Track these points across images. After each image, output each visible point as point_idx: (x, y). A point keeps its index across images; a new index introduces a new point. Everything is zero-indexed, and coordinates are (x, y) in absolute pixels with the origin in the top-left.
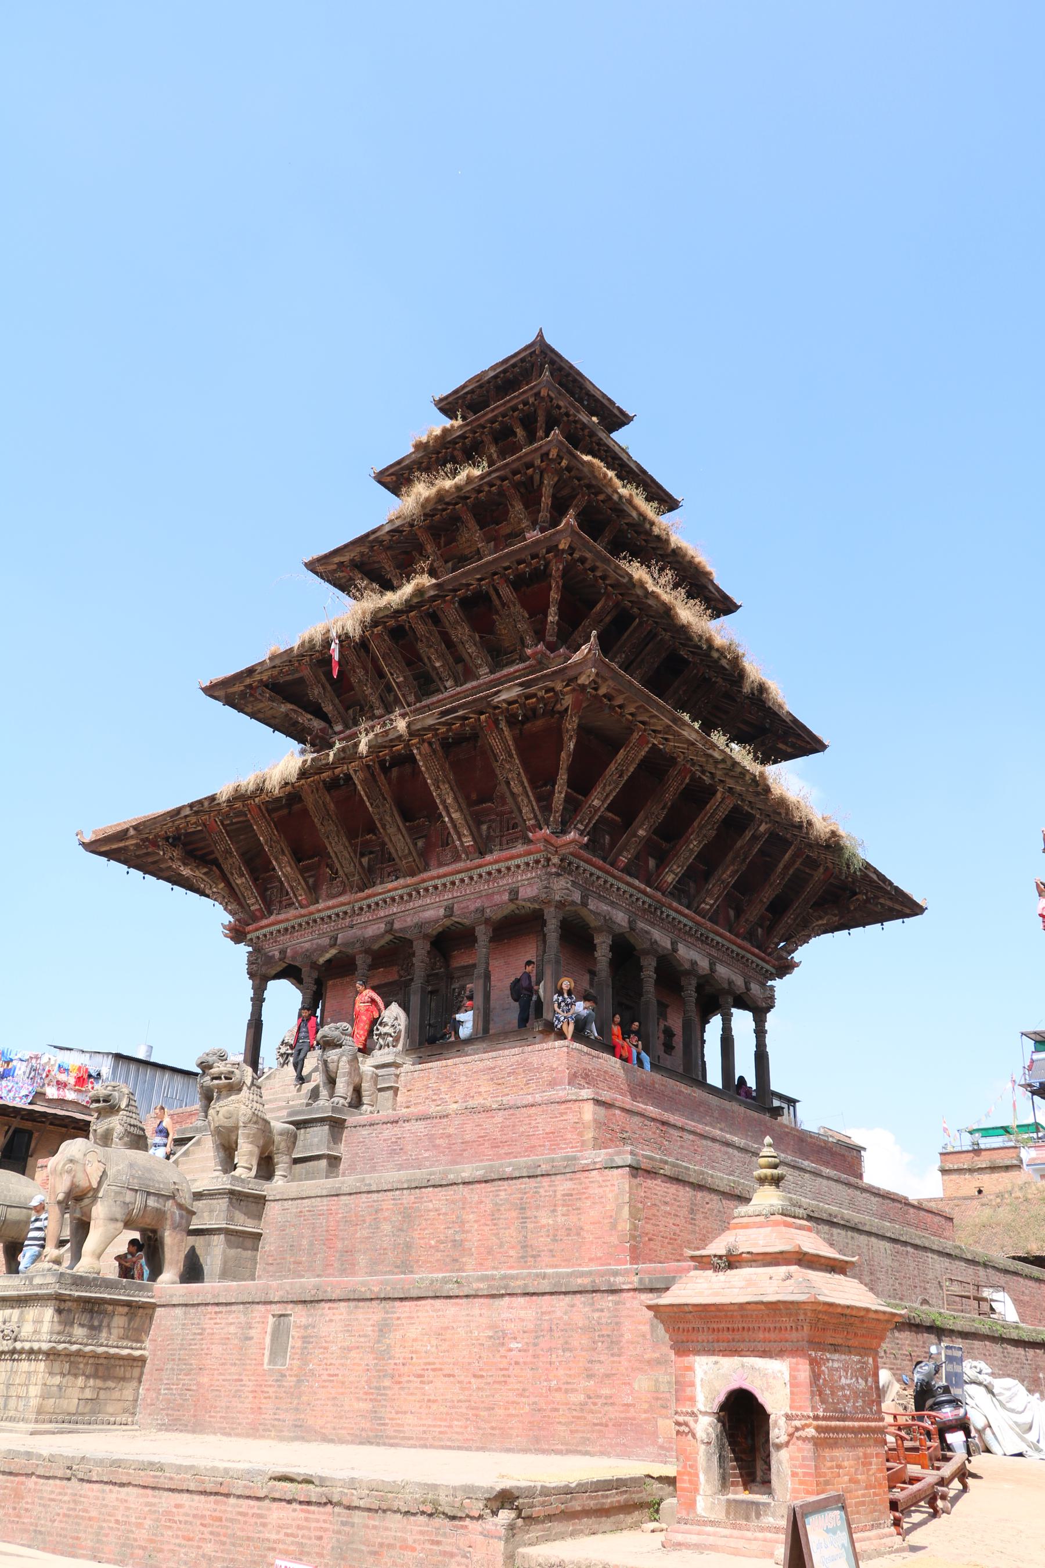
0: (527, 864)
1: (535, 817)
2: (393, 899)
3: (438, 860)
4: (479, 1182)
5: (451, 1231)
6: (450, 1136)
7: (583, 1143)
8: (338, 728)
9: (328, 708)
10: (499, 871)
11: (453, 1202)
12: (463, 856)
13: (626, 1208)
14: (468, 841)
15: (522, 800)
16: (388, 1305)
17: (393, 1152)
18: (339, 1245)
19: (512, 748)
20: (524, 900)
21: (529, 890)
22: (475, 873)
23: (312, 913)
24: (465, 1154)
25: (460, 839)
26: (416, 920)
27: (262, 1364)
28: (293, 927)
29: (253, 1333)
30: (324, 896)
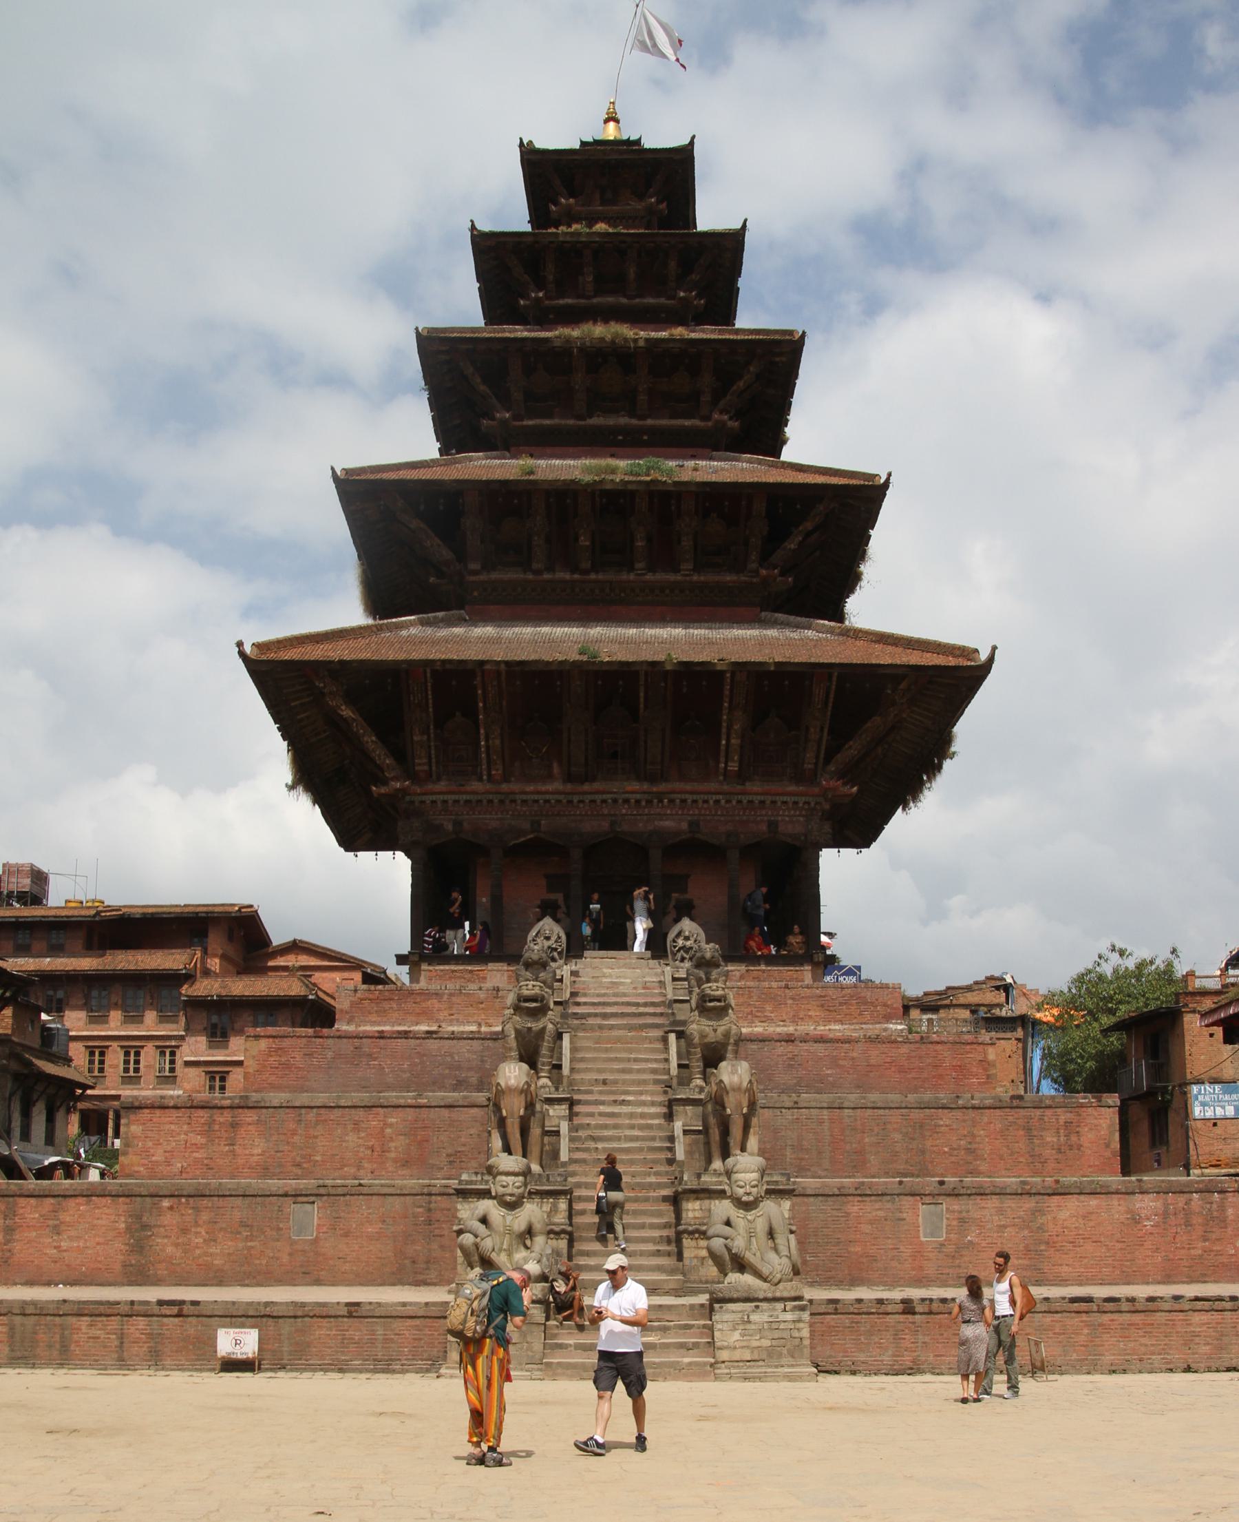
0: (796, 803)
1: (816, 764)
2: (626, 801)
4: (989, 1108)
7: (988, 1077)
10: (762, 802)
11: (964, 1121)
12: (721, 778)
13: (1117, 1134)
14: (734, 766)
16: (1038, 1197)
17: (791, 1066)
18: (848, 1147)
19: (831, 700)
23: (513, 793)
24: (872, 1075)
25: (726, 764)
26: (650, 827)
28: (480, 801)
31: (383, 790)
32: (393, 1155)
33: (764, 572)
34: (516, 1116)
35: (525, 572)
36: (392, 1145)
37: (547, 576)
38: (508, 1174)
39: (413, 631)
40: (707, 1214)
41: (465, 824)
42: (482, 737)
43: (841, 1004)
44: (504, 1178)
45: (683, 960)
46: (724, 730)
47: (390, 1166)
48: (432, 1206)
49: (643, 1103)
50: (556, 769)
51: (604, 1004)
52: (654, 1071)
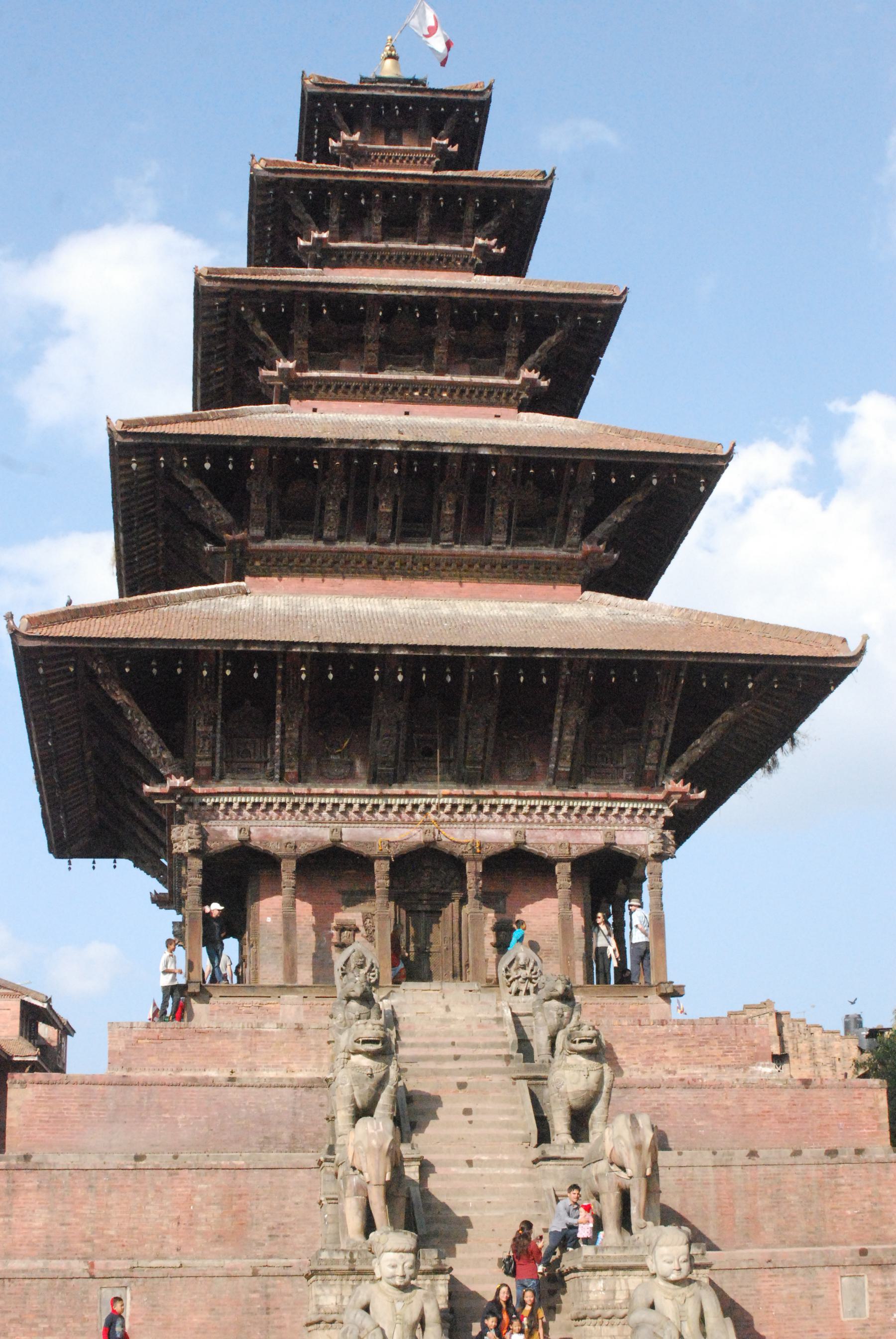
1: (658, 765)
3: (501, 771)
5: (867, 1204)
6: (727, 1108)
7: (879, 1126)
8: (259, 532)
9: (257, 505)
12: (551, 780)
14: (565, 767)
15: (654, 744)
20: (622, 846)
21: (628, 836)
22: (565, 805)
27: (839, 1317)
28: (269, 805)
29: (821, 1292)
30: (314, 771)
31: (157, 789)
32: (204, 1228)
33: (587, 547)
34: (382, 1182)
35: (315, 541)
36: (202, 1216)
37: (339, 545)
38: (396, 1251)
39: (193, 605)
40: (611, 1296)
41: (252, 830)
42: (278, 729)
43: (701, 1044)
44: (391, 1255)
45: (517, 993)
46: (556, 726)
47: (199, 1240)
48: (270, 1290)
49: (501, 1164)
50: (359, 767)
51: (435, 1045)
52: (508, 1125)
